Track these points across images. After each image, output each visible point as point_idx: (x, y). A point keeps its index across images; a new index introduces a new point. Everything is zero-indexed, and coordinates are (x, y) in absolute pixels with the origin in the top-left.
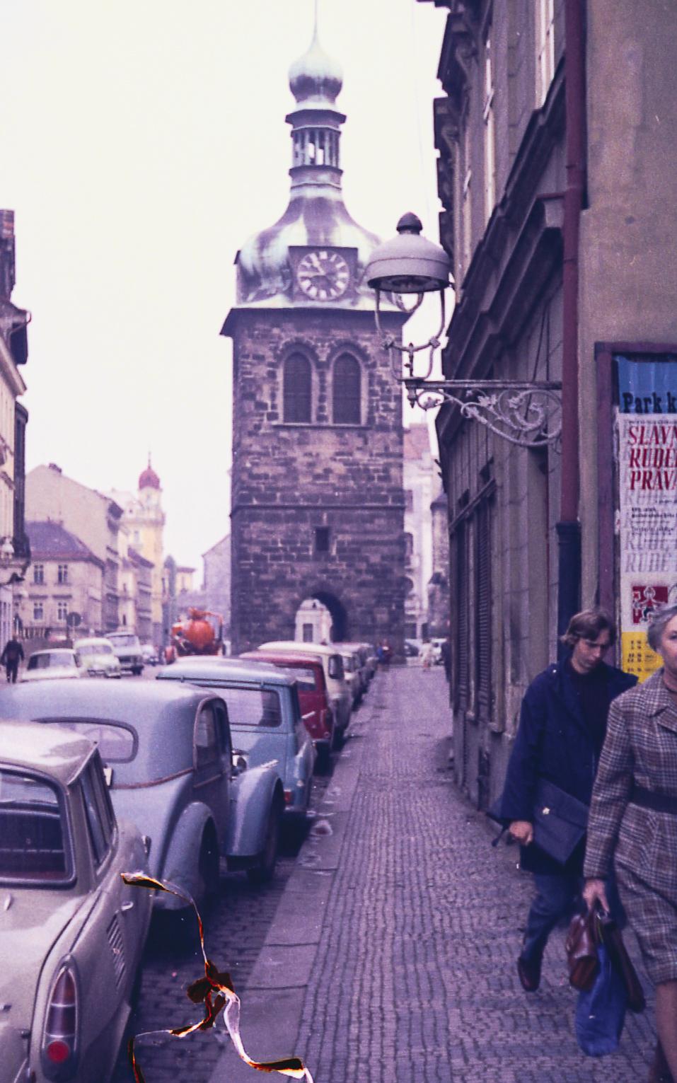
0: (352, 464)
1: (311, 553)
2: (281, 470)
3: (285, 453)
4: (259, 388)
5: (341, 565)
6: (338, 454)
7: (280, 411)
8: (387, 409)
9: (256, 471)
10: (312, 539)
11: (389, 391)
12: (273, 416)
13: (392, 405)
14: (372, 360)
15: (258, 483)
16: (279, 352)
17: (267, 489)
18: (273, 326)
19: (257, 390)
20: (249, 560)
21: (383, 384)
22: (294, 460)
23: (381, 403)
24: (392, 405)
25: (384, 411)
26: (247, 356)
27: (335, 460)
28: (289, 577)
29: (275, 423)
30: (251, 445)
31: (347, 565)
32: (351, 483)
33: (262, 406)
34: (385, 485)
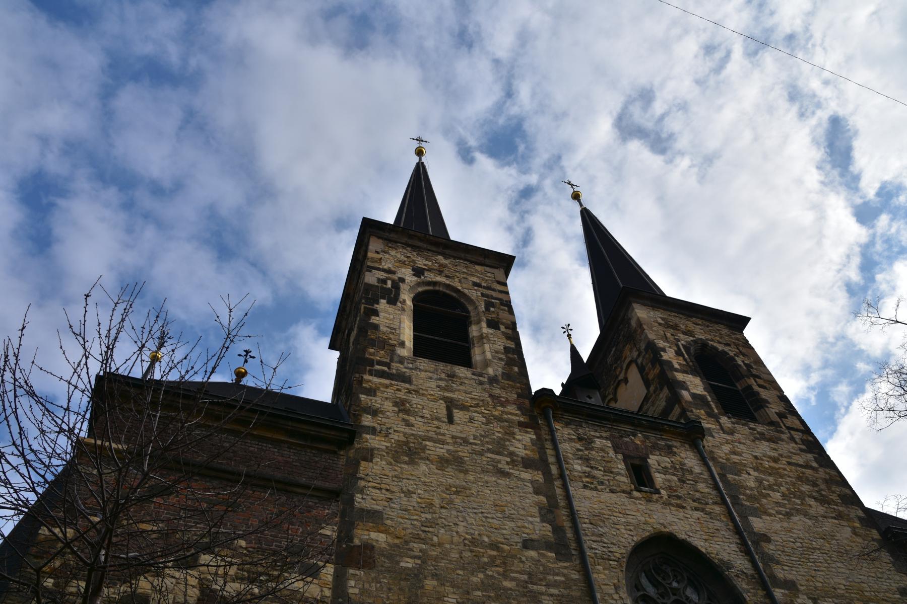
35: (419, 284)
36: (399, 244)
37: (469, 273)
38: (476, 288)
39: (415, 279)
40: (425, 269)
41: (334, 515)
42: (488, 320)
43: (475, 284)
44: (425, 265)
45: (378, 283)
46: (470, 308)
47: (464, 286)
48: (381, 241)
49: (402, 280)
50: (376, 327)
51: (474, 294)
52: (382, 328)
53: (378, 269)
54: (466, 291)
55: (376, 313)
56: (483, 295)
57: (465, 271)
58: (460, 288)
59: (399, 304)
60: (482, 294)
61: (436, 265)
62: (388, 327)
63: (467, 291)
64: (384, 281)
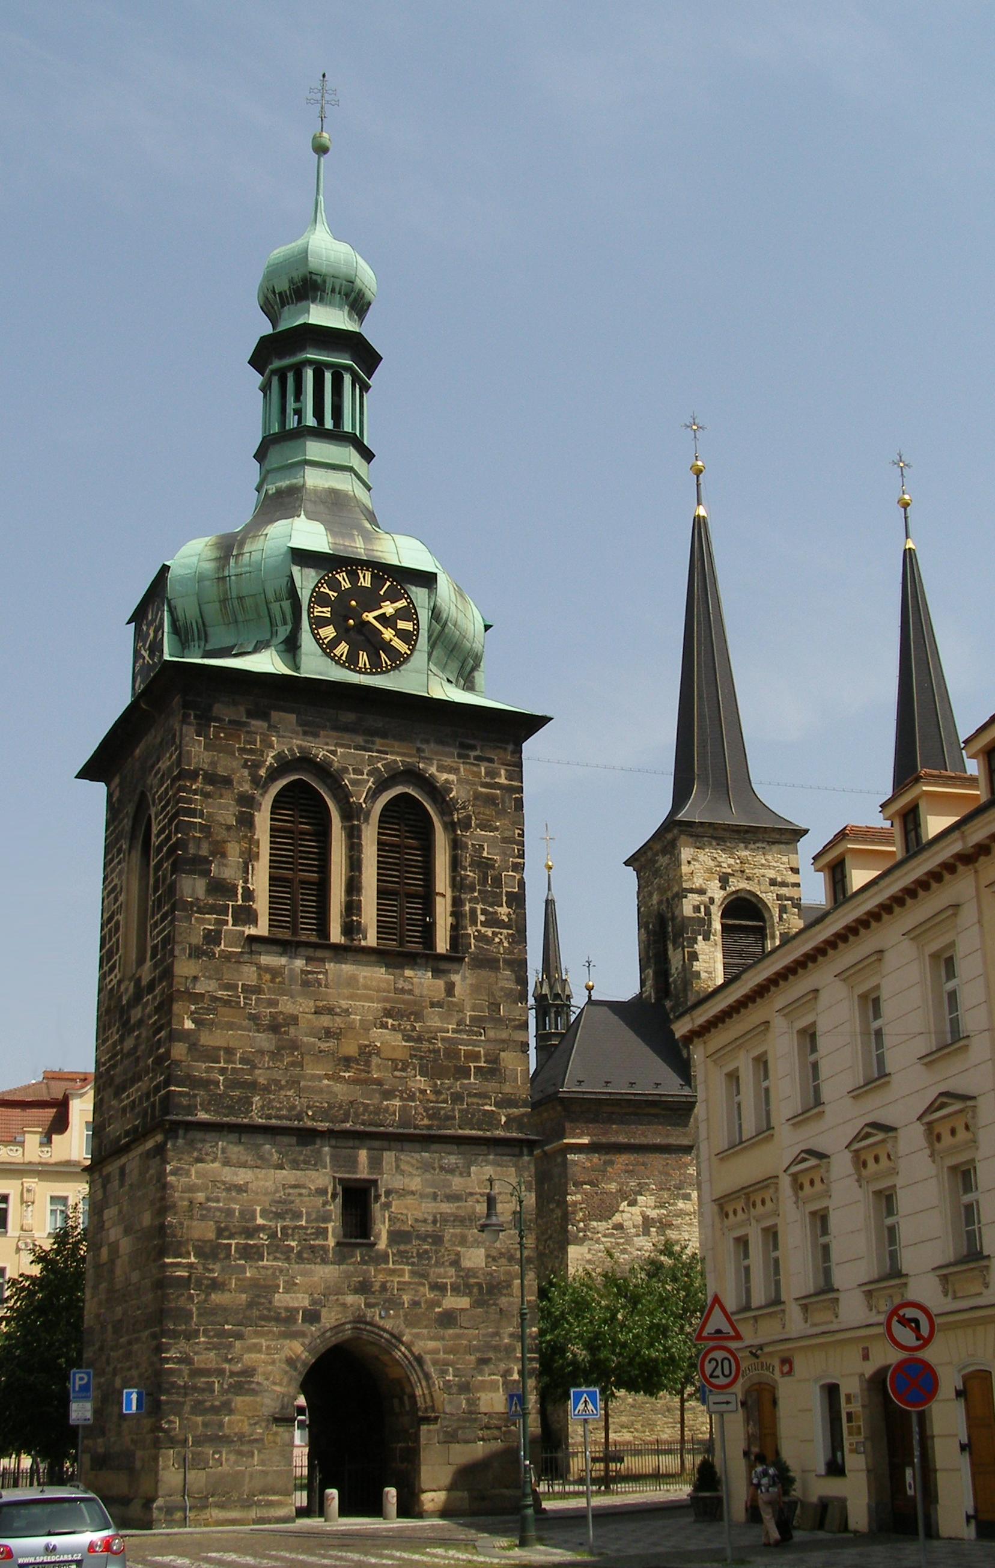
0: (419, 1039)
1: (331, 1242)
2: (265, 1040)
3: (273, 1003)
4: (219, 851)
5: (401, 1273)
6: (388, 1013)
7: (262, 905)
8: (493, 921)
9: (207, 1039)
10: (335, 1208)
11: (497, 881)
12: (246, 915)
13: (503, 911)
14: (463, 814)
15: (209, 1070)
16: (262, 772)
17: (232, 1084)
18: (250, 714)
19: (213, 854)
20: (188, 1255)
21: (483, 865)
22: (294, 1020)
23: (479, 907)
24: (503, 911)
25: (483, 924)
26: (193, 775)
27: (384, 1026)
28: (282, 1299)
29: (250, 930)
30: (195, 978)
31: (413, 1273)
32: (420, 1082)
33: (221, 888)
34: (491, 1086)
35: (725, 898)
36: (706, 839)
37: (767, 864)
38: (772, 888)
39: (722, 892)
40: (730, 874)
41: (692, 1161)
42: (780, 933)
43: (773, 882)
44: (729, 866)
45: (694, 912)
46: (766, 916)
47: (763, 888)
48: (691, 840)
49: (712, 900)
50: (697, 975)
51: (769, 897)
52: (703, 975)
53: (692, 891)
54: (762, 896)
55: (694, 956)
56: (779, 897)
57: (764, 862)
58: (758, 893)
59: (712, 937)
60: (777, 895)
61: (738, 861)
62: (706, 972)
63: (764, 895)
64: (697, 909)
